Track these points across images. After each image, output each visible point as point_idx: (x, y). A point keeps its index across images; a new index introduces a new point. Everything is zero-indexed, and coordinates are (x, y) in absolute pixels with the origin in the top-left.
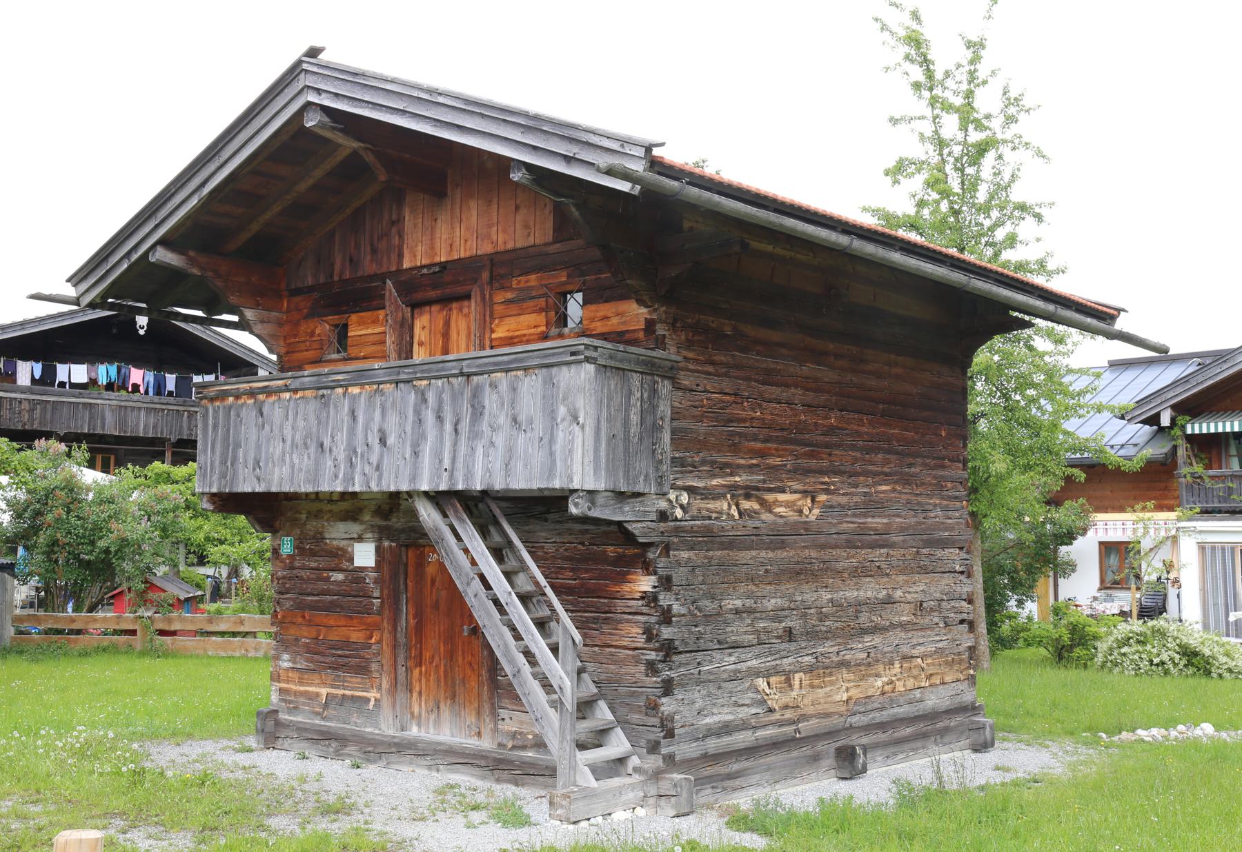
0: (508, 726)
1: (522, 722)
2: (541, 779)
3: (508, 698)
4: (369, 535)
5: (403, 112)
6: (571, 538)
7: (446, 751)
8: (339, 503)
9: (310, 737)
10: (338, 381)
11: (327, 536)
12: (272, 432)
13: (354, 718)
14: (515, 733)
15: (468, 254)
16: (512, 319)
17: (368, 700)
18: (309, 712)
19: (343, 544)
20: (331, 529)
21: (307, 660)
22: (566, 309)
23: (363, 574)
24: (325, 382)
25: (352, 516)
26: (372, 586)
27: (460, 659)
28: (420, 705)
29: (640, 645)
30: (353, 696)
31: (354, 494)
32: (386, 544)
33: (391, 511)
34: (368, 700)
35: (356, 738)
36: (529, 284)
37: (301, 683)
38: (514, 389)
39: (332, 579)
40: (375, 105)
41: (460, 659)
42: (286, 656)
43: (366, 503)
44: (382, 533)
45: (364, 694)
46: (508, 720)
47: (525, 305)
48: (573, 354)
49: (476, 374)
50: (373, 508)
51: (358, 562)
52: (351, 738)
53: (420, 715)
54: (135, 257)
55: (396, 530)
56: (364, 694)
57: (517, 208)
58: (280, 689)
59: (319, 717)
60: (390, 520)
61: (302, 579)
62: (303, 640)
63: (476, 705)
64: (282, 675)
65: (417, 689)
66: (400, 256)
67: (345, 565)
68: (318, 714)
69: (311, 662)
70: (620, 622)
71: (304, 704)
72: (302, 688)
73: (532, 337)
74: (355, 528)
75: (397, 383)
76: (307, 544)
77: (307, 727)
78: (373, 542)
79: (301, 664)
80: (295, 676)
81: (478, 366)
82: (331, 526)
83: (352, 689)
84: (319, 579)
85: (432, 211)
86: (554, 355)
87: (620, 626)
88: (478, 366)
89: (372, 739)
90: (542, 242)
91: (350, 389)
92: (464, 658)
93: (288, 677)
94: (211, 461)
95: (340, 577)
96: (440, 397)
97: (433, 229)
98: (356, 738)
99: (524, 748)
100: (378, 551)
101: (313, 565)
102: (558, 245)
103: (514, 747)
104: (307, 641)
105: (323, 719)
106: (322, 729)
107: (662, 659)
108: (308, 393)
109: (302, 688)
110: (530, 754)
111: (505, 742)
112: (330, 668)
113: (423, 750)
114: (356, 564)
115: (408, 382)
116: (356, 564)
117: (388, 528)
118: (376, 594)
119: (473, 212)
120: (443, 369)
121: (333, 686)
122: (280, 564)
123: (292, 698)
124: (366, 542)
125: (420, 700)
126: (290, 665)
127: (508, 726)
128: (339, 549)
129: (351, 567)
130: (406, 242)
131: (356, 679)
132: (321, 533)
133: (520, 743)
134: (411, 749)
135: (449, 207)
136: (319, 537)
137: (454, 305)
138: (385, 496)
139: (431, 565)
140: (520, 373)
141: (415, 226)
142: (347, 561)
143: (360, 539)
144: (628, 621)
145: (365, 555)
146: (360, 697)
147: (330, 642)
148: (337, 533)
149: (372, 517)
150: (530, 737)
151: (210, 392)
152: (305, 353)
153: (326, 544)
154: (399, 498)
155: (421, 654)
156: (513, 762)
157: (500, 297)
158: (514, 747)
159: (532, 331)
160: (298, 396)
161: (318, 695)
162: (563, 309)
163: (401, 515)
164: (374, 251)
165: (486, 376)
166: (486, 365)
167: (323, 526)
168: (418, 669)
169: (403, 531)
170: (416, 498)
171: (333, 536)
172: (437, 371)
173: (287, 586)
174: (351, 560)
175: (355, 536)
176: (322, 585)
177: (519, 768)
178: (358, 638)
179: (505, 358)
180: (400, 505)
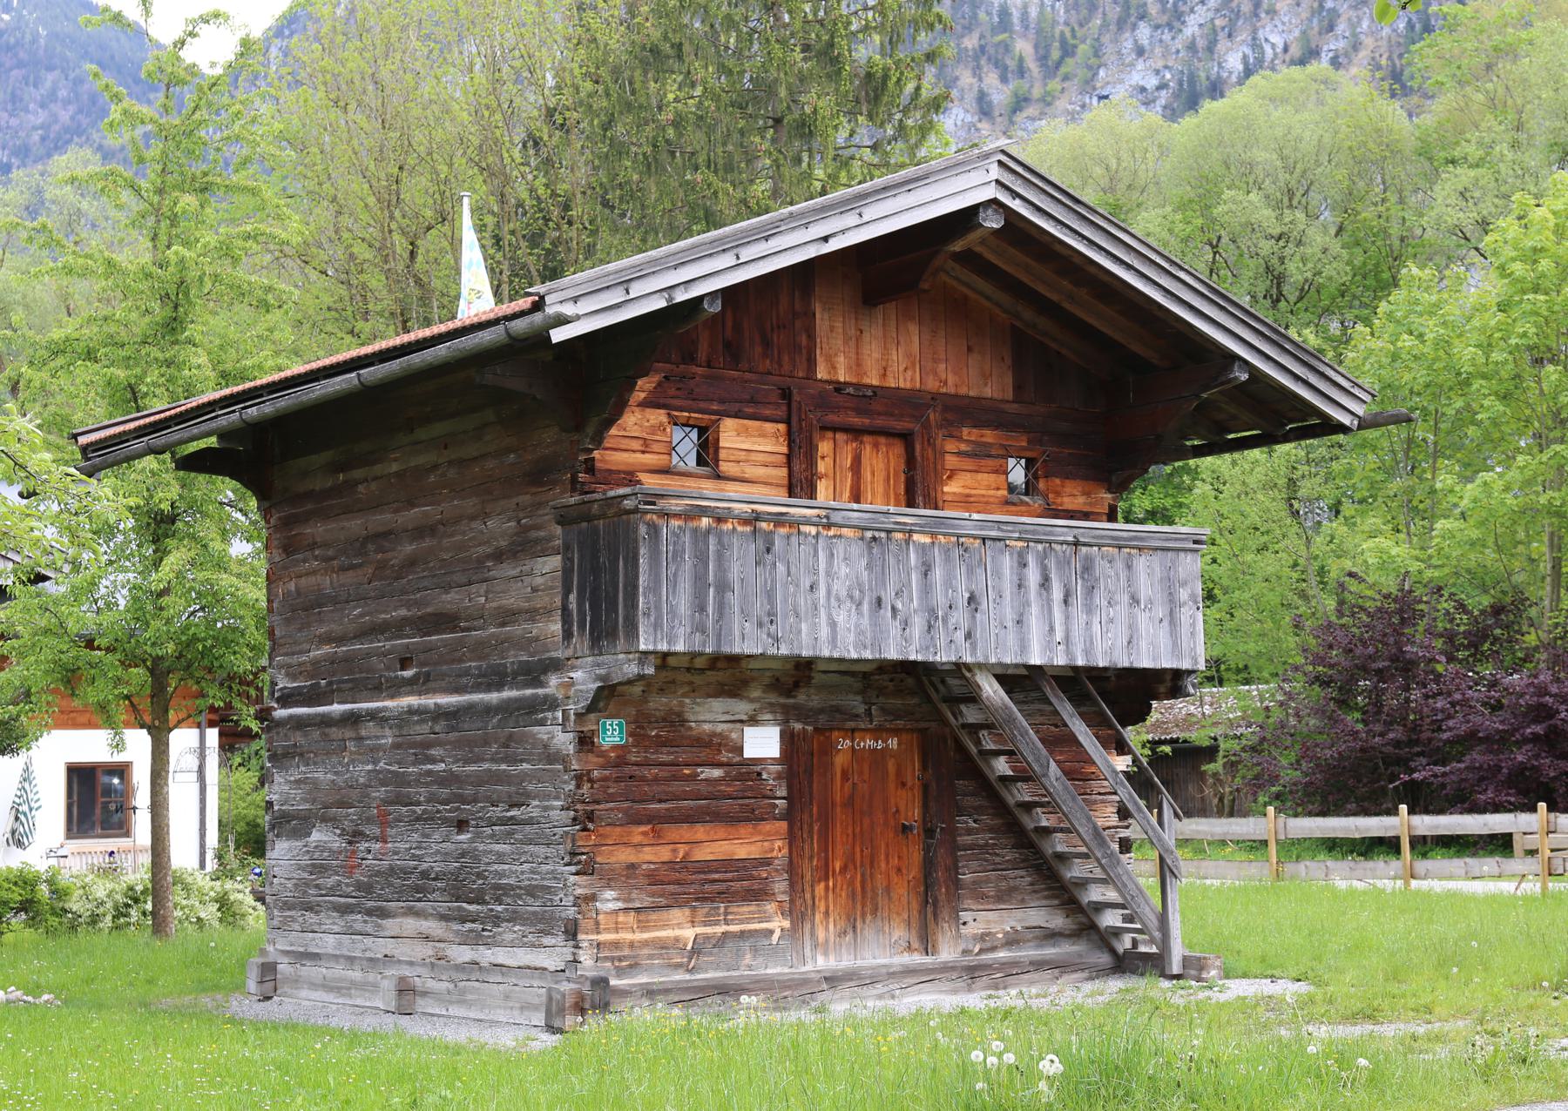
0: (972, 929)
1: (988, 922)
2: (1026, 976)
3: (971, 898)
4: (768, 716)
5: (1129, 267)
6: (1041, 719)
7: (902, 972)
8: (709, 673)
9: (676, 999)
10: (905, 524)
11: (692, 718)
12: (789, 575)
13: (748, 959)
14: (983, 934)
15: (908, 386)
16: (968, 474)
17: (771, 932)
18: (662, 966)
19: (720, 728)
20: (697, 709)
21: (653, 896)
22: (1026, 476)
23: (758, 768)
24: (883, 523)
25: (733, 690)
26: (771, 782)
27: (883, 865)
28: (827, 929)
29: (1115, 824)
30: (742, 932)
31: (735, 659)
32: (798, 726)
33: (796, 685)
34: (771, 932)
35: (762, 985)
36: (984, 439)
37: (643, 927)
38: (1129, 567)
39: (702, 776)
40: (1091, 243)
41: (883, 865)
42: (609, 894)
43: (755, 674)
44: (785, 716)
45: (764, 925)
46: (972, 922)
47: (983, 462)
48: (1195, 542)
49: (1085, 545)
50: (767, 681)
51: (749, 753)
52: (751, 986)
53: (827, 941)
54: (681, 297)
55: (811, 710)
56: (764, 925)
57: (969, 349)
58: (598, 945)
59: (681, 971)
60: (795, 697)
61: (643, 779)
62: (644, 867)
63: (906, 917)
64: (602, 922)
65: (822, 909)
66: (811, 363)
67: (725, 756)
68: (678, 966)
69: (661, 896)
70: (1095, 802)
71: (651, 957)
72: (646, 936)
73: (991, 500)
74: (742, 708)
75: (984, 539)
76: (652, 729)
77: (665, 986)
78: (774, 725)
79: (642, 900)
80: (631, 918)
81: (1093, 537)
82: (698, 704)
83: (741, 922)
84: (675, 778)
85: (856, 319)
86: (1176, 539)
87: (1094, 807)
88: (1093, 537)
89: (789, 980)
90: (1000, 397)
91: (915, 537)
92: (888, 863)
93: (617, 923)
94: (702, 609)
95: (717, 773)
96: (1042, 563)
97: (858, 340)
98: (762, 985)
99: (993, 949)
100: (788, 739)
101: (664, 758)
102: (1016, 406)
103: (981, 951)
104: (652, 867)
105: (690, 971)
106: (695, 984)
107: (279, 925)
108: (845, 531)
109: (646, 936)
110: (1001, 955)
111: (970, 947)
112: (697, 899)
113: (871, 977)
114: (748, 753)
115: (1000, 540)
116: (748, 753)
117: (796, 707)
118: (782, 792)
119: (914, 337)
120: (953, 527)
121: (705, 924)
122: (596, 760)
123: (626, 952)
124: (763, 725)
125: (828, 923)
126: (620, 905)
127: (972, 929)
128: (714, 734)
129: (738, 759)
130: (818, 346)
131: (746, 909)
132: (679, 714)
133: (989, 945)
134: (852, 980)
135: (880, 321)
136: (676, 720)
137: (867, 439)
138: (788, 666)
139: (841, 754)
140: (1134, 551)
141: (832, 329)
142: (729, 751)
143: (753, 721)
144: (1103, 802)
145: (762, 743)
146: (756, 931)
147: (697, 865)
148: (709, 715)
149: (764, 692)
150: (1000, 936)
151: (671, 505)
152: (639, 455)
153: (690, 728)
154: (811, 669)
155: (827, 865)
156: (990, 966)
157: (951, 446)
158: (981, 951)
159: (992, 492)
160: (831, 533)
161: (677, 939)
162: (1030, 476)
163: (812, 691)
164: (767, 344)
165: (1096, 549)
166: (1103, 537)
167: (682, 704)
168: (822, 885)
169: (822, 711)
170: (977, 671)
171: (702, 718)
172: (1045, 534)
173: (611, 791)
174: (740, 750)
175: (744, 718)
176: (676, 787)
177: (998, 970)
178: (749, 854)
179: (1125, 534)
180: (810, 678)
